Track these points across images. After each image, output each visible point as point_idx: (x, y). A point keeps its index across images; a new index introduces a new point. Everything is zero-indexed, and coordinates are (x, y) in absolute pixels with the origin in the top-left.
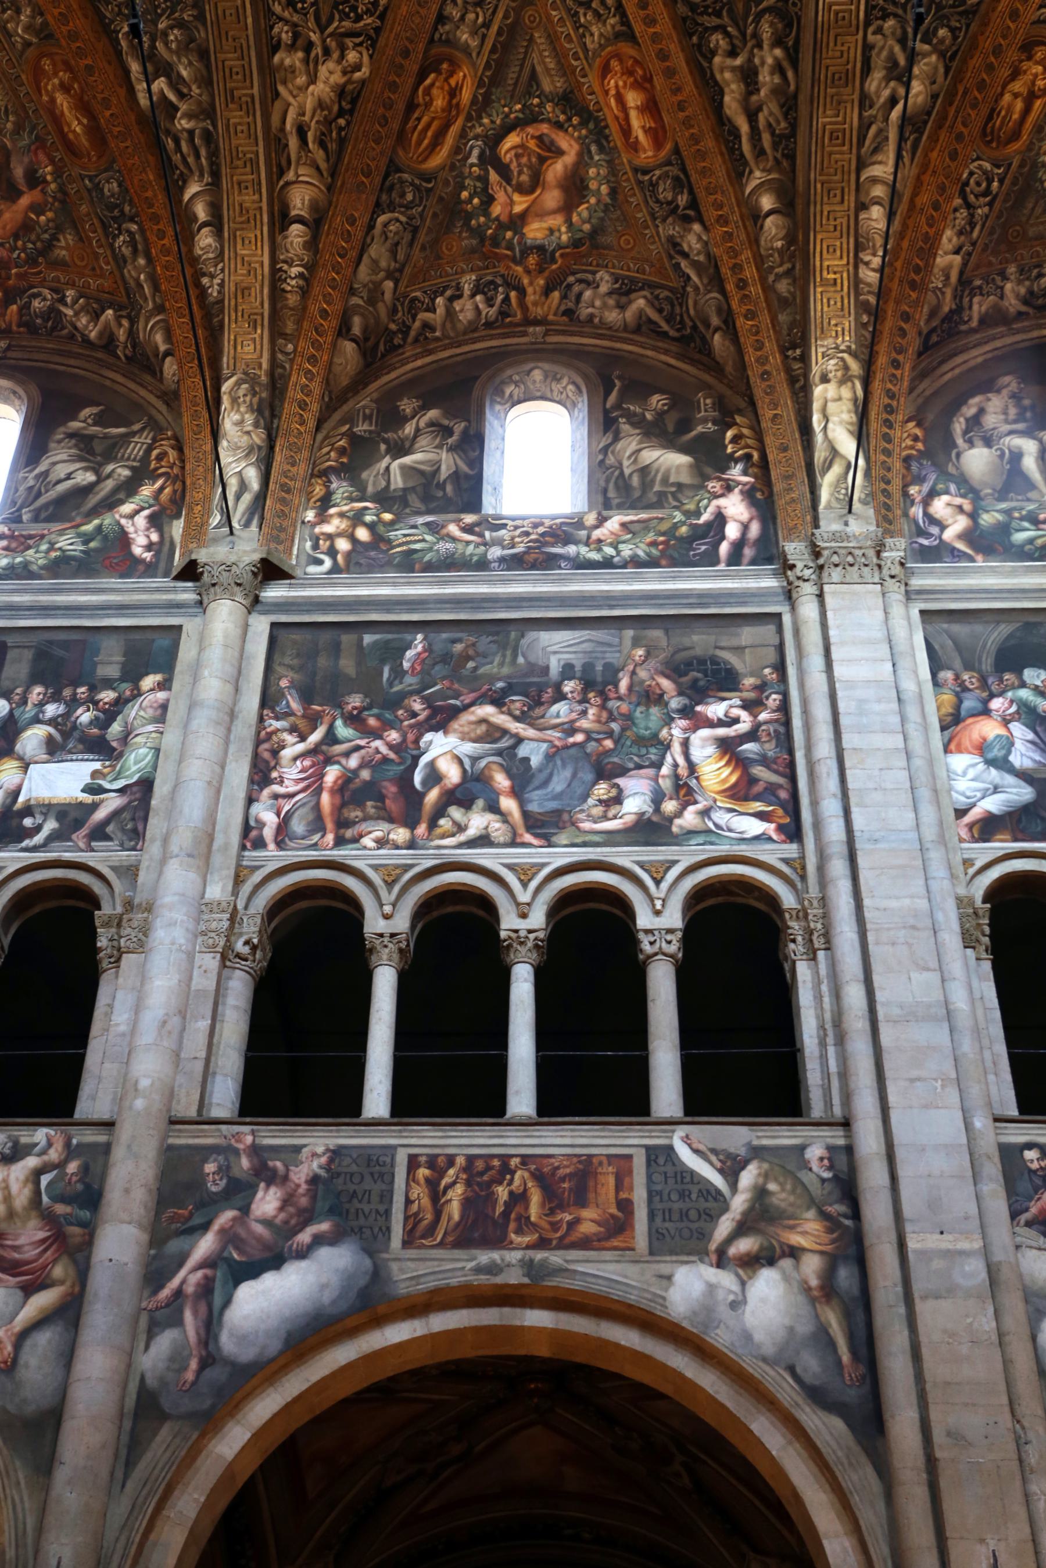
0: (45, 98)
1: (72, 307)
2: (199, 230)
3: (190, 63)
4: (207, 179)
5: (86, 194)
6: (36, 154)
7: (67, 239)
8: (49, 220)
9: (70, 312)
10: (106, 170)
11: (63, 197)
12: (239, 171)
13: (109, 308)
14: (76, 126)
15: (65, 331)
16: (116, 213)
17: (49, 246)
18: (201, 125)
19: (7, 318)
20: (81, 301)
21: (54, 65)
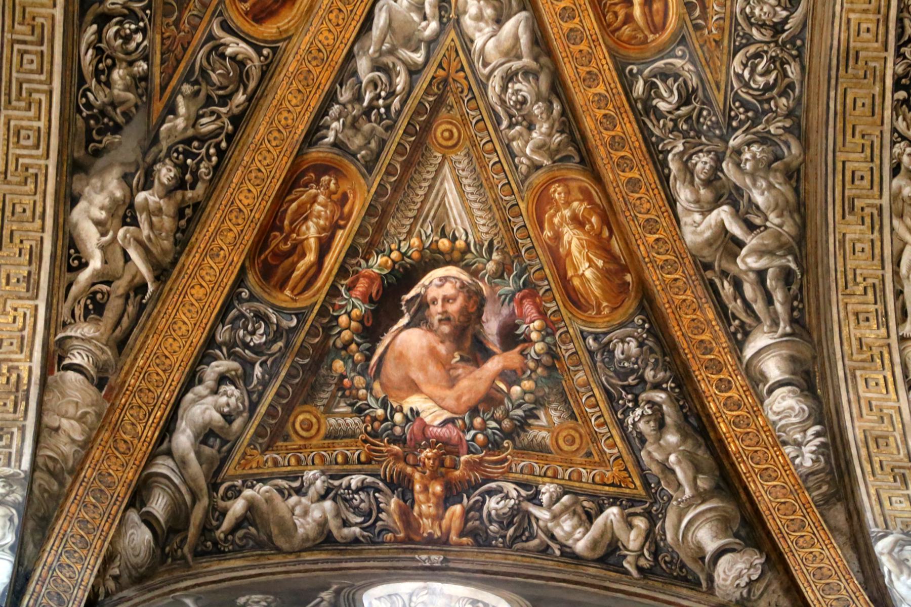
0: (548, 233)
1: (549, 508)
2: (771, 391)
3: (771, 186)
4: (784, 327)
5: (585, 358)
6: (520, 303)
7: (551, 417)
8: (525, 392)
9: (543, 514)
10: (621, 326)
11: (552, 362)
12: (854, 300)
13: (612, 505)
14: (586, 269)
15: (536, 542)
16: (631, 380)
17: (523, 425)
18: (778, 262)
19: (445, 523)
20: (565, 499)
21: (568, 193)
